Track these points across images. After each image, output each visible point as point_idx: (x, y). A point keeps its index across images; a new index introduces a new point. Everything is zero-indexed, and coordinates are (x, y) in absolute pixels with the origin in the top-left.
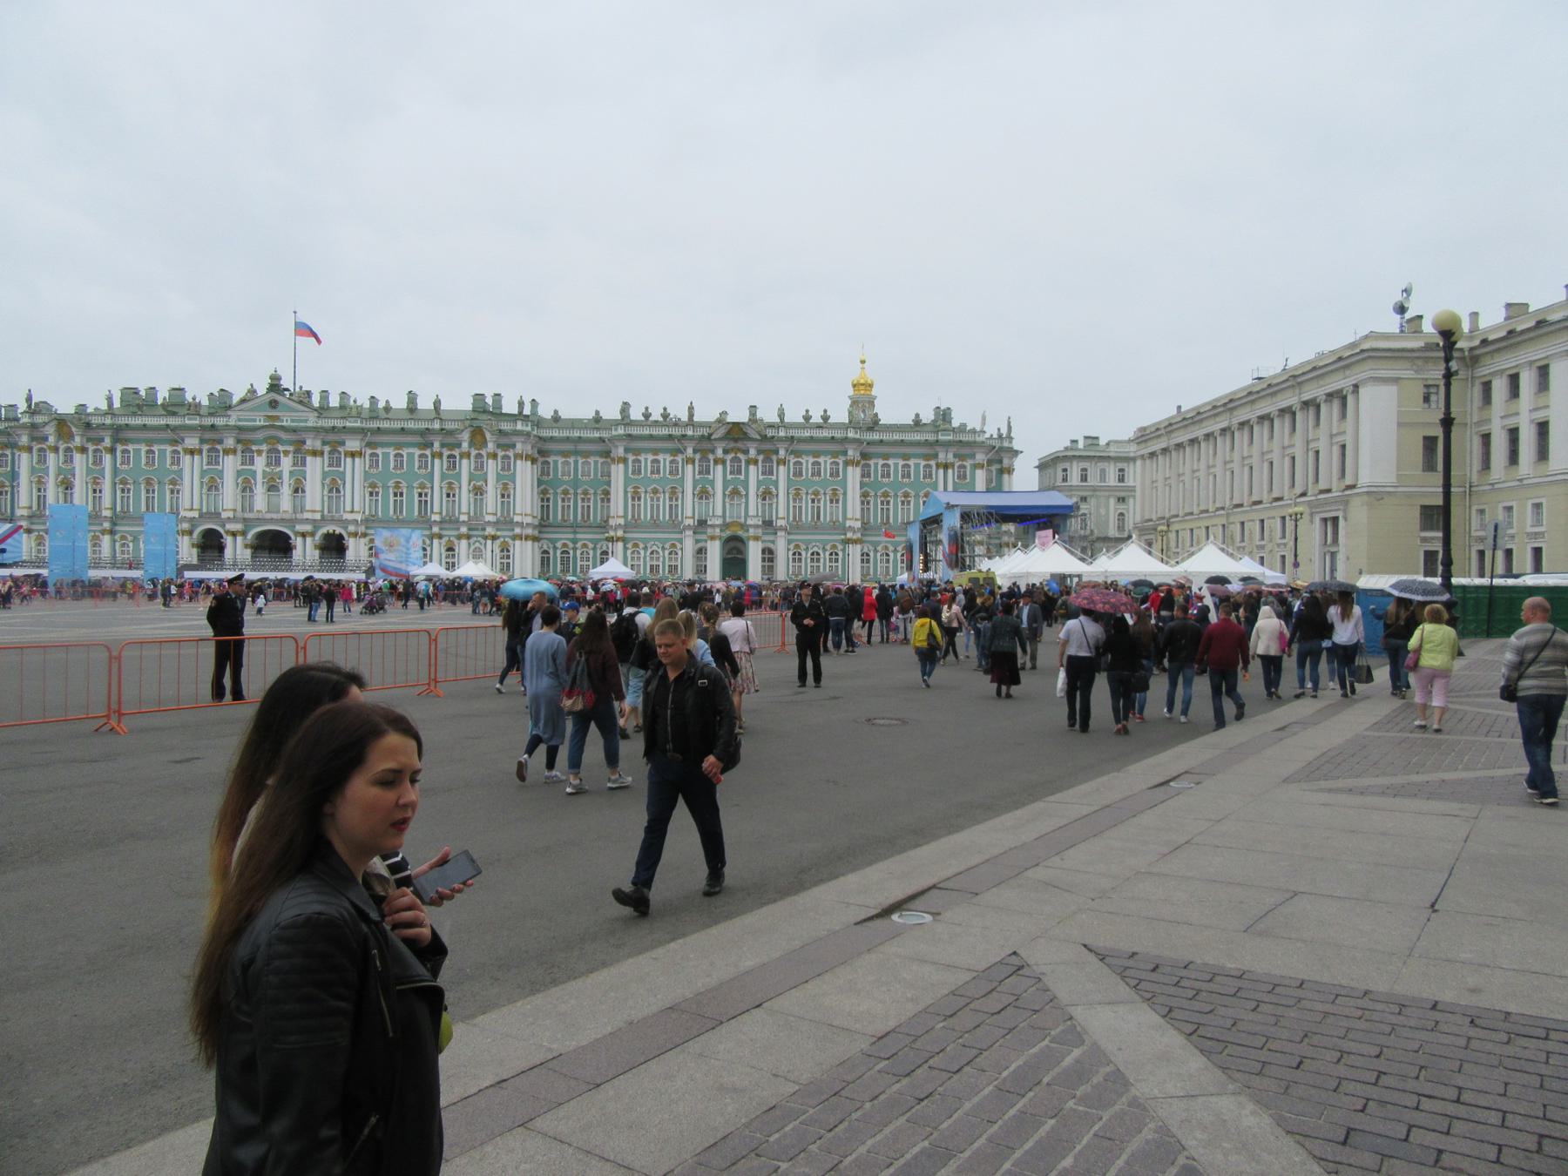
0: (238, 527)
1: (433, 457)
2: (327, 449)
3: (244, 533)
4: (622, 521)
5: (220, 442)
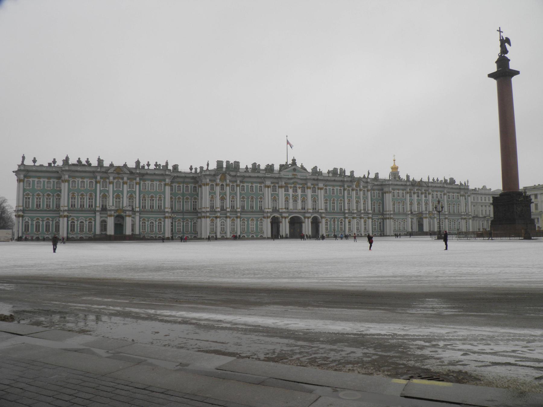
0: (286, 215)
1: (344, 190)
2: (312, 186)
3: (288, 217)
4: (392, 212)
5: (278, 183)
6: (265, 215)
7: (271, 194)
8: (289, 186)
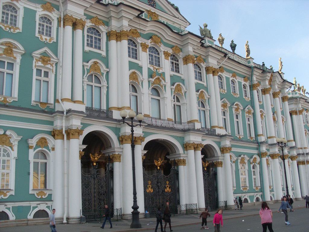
1: (252, 87)
6: (60, 123)
7: (84, 53)
8: (140, 40)
